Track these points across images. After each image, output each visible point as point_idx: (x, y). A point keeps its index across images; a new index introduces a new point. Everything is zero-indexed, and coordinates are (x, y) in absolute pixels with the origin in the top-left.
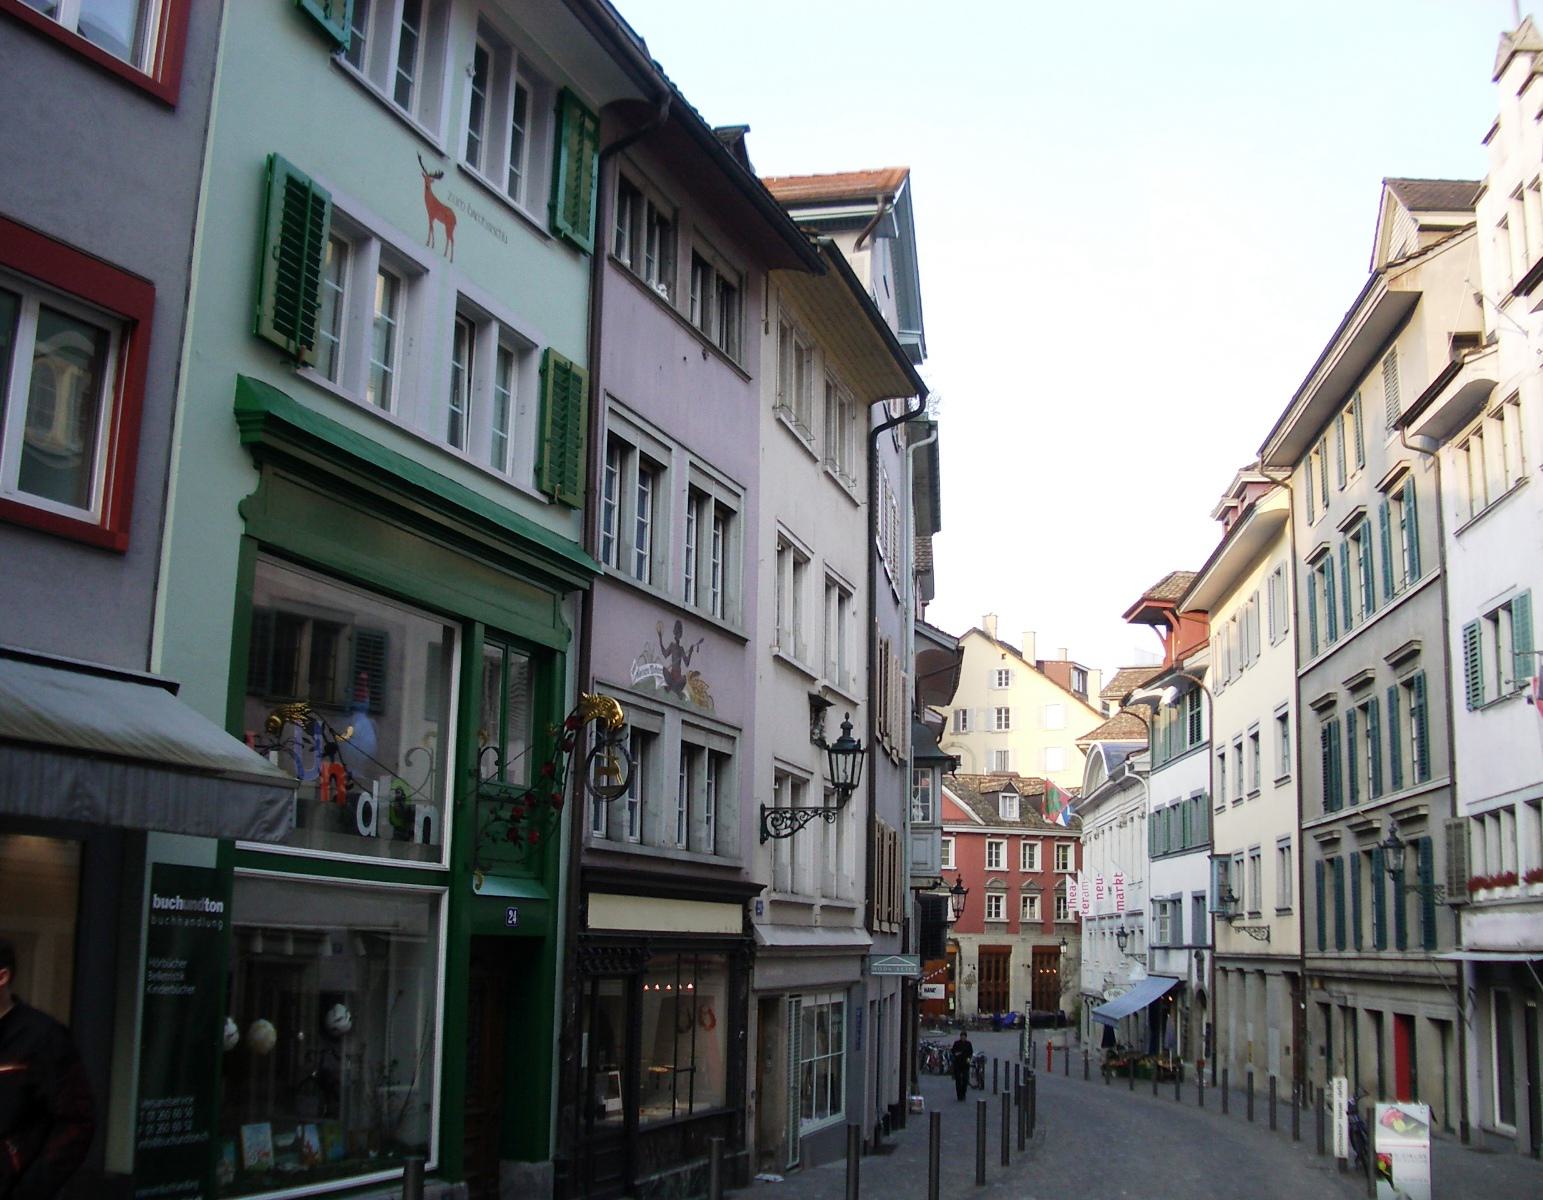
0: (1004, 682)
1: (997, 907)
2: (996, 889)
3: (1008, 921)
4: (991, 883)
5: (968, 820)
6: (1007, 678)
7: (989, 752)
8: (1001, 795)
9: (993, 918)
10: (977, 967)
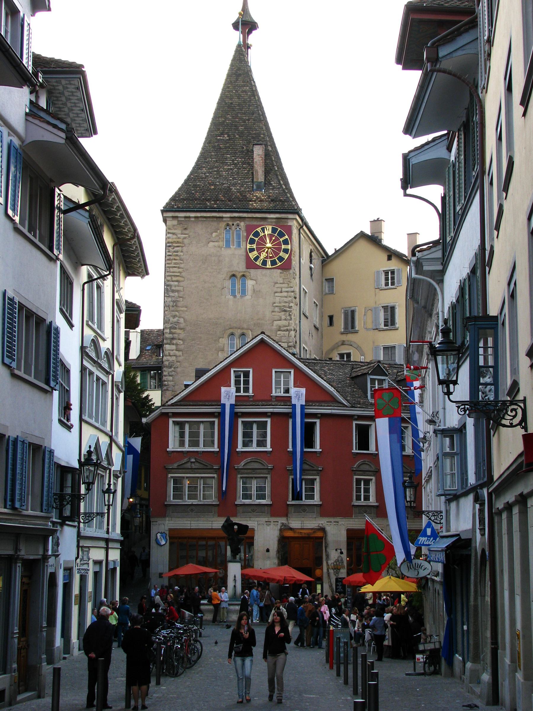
0: (390, 281)
1: (367, 491)
2: (364, 472)
3: (376, 504)
4: (359, 466)
5: (334, 401)
6: (393, 278)
7: (377, 348)
8: (369, 378)
9: (362, 502)
10: (345, 551)
